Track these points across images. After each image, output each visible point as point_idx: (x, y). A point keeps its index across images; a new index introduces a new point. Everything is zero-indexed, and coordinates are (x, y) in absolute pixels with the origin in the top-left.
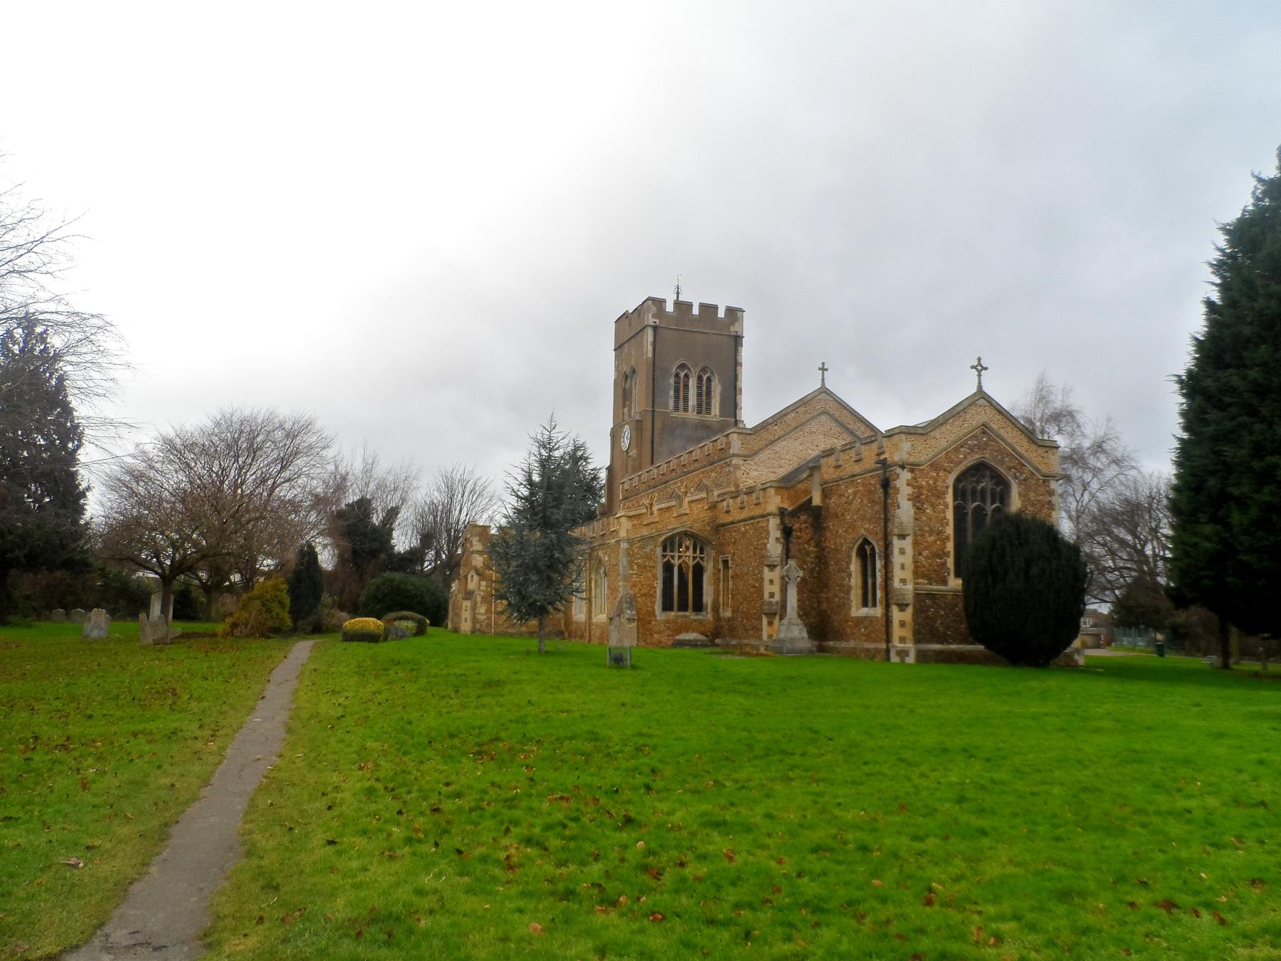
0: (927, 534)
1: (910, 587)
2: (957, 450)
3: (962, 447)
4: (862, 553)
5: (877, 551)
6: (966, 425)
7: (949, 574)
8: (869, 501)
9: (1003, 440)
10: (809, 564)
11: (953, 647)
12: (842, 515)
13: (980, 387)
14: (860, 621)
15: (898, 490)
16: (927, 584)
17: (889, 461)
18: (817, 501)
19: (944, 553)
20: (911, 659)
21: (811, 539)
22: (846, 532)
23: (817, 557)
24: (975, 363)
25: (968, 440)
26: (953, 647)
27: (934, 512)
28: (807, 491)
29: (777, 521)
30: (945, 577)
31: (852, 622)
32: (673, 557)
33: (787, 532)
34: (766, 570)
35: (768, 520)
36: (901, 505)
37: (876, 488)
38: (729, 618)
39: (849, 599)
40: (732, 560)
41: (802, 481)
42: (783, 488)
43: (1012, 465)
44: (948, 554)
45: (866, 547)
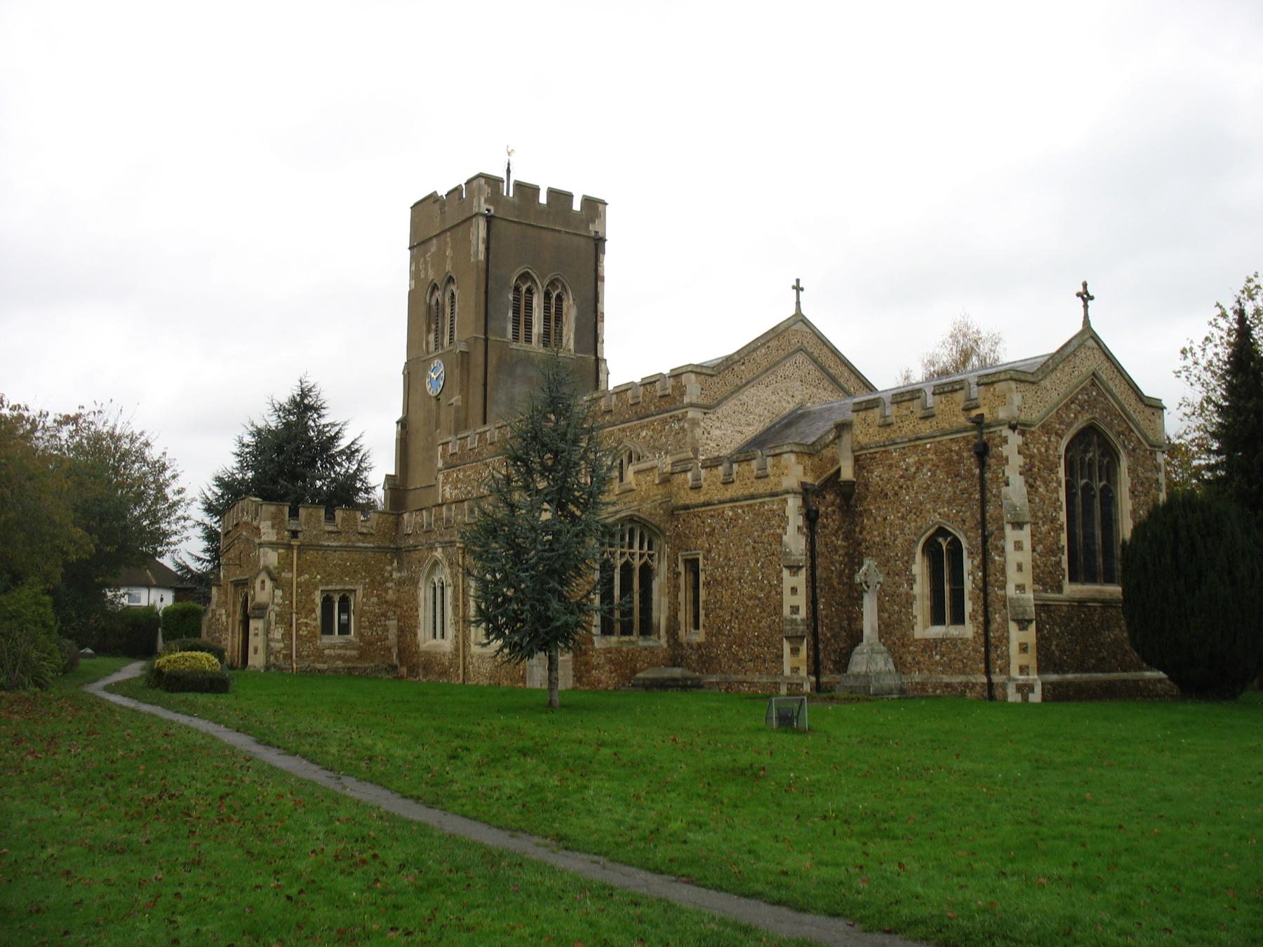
0: (1041, 522)
1: (1029, 595)
2: (1067, 406)
3: (1073, 402)
4: (932, 549)
5: (964, 544)
6: (1076, 373)
7: (1064, 578)
8: (948, 473)
9: (1113, 395)
10: (837, 565)
11: (1070, 676)
12: (896, 494)
13: (1086, 321)
14: (930, 645)
15: (1007, 459)
16: (1042, 591)
17: (988, 418)
18: (847, 473)
19: (1058, 548)
20: (1036, 697)
21: (839, 529)
22: (903, 518)
23: (846, 554)
24: (1081, 289)
25: (1078, 393)
26: (1070, 676)
27: (1047, 491)
28: (834, 461)
29: (799, 502)
30: (1060, 581)
31: (916, 646)
32: (612, 554)
33: (811, 518)
34: (786, 573)
35: (785, 501)
36: (1011, 481)
37: (961, 457)
38: (700, 645)
39: (909, 613)
40: (705, 558)
41: (827, 446)
42: (806, 453)
43: (1120, 429)
44: (1061, 549)
45: (940, 540)
